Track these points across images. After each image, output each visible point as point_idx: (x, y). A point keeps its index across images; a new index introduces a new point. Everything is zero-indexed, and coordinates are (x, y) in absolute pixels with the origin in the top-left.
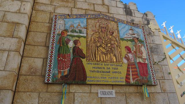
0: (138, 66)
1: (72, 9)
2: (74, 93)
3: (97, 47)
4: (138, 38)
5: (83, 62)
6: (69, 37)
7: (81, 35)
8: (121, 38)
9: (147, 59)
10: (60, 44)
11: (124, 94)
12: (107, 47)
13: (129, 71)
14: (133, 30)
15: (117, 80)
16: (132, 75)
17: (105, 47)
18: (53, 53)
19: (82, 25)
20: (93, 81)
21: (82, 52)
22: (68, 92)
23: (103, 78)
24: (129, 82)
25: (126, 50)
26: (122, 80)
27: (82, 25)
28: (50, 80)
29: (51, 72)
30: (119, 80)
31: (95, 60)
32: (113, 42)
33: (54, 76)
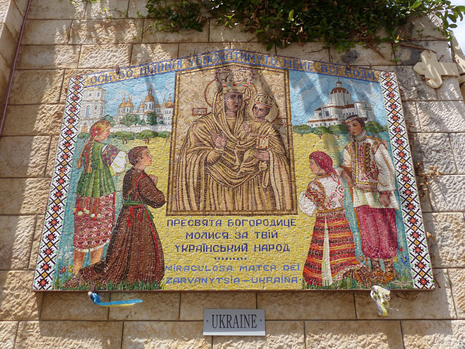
0: (358, 221)
1: (135, 46)
2: (124, 321)
3: (206, 164)
5: (154, 220)
6: (113, 142)
8: (296, 127)
10: (86, 163)
11: (298, 323)
12: (241, 160)
13: (321, 243)
14: (344, 90)
16: (332, 254)
17: (235, 161)
18: (63, 198)
20: (183, 280)
21: (155, 186)
22: (105, 319)
23: (222, 268)
24: (319, 282)
29: (53, 255)
30: (279, 272)
31: (195, 208)
32: (264, 143)
33: (62, 270)
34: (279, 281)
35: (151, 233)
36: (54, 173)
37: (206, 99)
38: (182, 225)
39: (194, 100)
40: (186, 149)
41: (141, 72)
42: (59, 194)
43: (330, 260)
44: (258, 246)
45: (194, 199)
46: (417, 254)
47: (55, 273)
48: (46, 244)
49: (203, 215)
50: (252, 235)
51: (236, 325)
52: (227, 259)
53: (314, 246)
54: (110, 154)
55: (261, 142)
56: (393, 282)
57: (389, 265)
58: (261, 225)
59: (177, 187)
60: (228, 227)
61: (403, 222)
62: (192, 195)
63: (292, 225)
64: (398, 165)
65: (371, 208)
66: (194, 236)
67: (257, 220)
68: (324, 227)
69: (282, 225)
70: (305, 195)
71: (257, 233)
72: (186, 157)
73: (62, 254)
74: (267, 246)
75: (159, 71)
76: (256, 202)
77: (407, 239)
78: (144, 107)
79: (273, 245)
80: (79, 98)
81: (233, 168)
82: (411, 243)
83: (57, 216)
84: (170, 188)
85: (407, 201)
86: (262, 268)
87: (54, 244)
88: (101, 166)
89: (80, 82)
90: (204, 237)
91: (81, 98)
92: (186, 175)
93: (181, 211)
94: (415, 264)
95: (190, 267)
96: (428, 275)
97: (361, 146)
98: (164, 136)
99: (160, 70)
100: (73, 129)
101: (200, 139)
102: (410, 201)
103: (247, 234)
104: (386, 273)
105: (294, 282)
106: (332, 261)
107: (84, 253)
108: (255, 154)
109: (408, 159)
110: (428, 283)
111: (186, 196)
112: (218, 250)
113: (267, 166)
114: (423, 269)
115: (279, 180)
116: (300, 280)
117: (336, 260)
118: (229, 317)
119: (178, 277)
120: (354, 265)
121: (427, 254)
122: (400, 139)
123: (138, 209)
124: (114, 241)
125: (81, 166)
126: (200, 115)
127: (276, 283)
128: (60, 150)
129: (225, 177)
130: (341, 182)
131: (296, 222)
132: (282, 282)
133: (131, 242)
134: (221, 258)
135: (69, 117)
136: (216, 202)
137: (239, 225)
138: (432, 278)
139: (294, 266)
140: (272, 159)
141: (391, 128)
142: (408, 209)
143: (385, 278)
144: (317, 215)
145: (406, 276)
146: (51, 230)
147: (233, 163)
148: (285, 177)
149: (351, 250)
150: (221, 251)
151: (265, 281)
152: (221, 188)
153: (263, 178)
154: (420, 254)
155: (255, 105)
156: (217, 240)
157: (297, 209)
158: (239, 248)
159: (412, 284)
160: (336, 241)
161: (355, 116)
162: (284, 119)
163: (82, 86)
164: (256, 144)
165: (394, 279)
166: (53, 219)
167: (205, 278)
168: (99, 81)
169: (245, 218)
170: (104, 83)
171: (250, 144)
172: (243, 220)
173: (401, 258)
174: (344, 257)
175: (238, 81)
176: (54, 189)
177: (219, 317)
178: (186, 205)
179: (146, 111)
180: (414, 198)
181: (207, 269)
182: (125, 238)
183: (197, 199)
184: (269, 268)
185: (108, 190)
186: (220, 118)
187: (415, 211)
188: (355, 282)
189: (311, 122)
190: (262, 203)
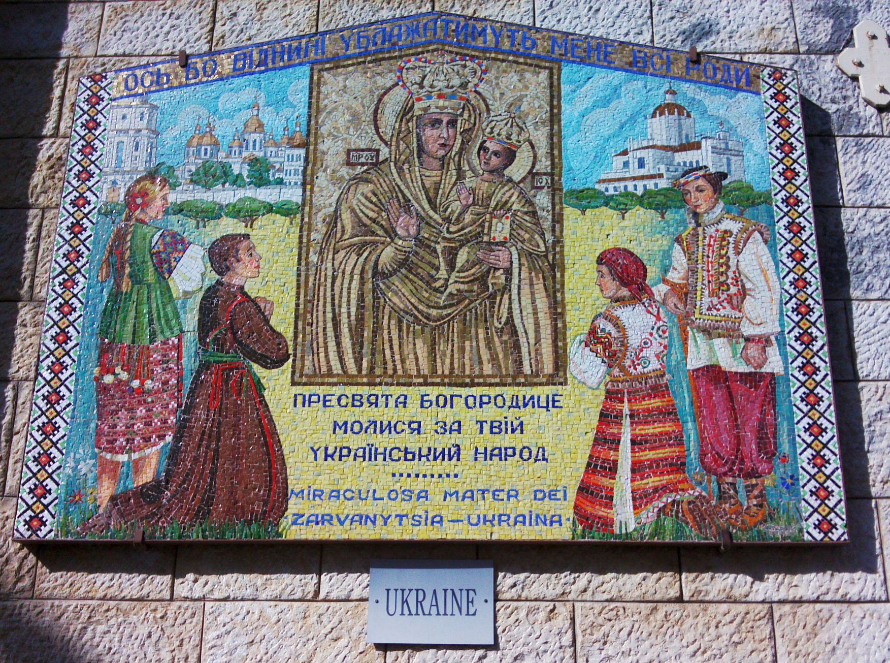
3: (375, 274)
4: (724, 176)
5: (266, 393)
6: (175, 223)
7: (266, 195)
8: (572, 192)
9: (781, 339)
10: (118, 273)
12: (451, 266)
13: (615, 442)
14: (681, 109)
15: (512, 508)
16: (637, 469)
17: (437, 269)
19: (274, 122)
21: (267, 321)
23: (408, 494)
24: (607, 523)
25: (608, 279)
26: (547, 507)
27: (274, 122)
28: (44, 524)
30: (524, 505)
33: (74, 496)
34: (524, 523)
35: (260, 421)
36: (50, 292)
37: (377, 128)
38: (325, 406)
39: (351, 131)
40: (333, 242)
41: (235, 64)
42: (62, 338)
43: (632, 481)
44: (481, 450)
45: (350, 351)
46: (816, 470)
47: (60, 502)
48: (39, 443)
49: (369, 384)
50: (469, 427)
51: (434, 609)
52: (417, 476)
53: (600, 452)
54: (169, 250)
55: (493, 228)
56: (762, 528)
57: (756, 492)
58: (490, 405)
59: (314, 326)
60: (420, 410)
61: (790, 401)
62: (346, 342)
63: (554, 406)
64: (787, 280)
65: (725, 372)
66: (349, 429)
67: (481, 397)
68: (621, 410)
69: (533, 407)
70: (583, 344)
71: (481, 423)
72: (333, 259)
73: (73, 464)
74: (500, 449)
75: (274, 63)
76: (480, 358)
77: (798, 439)
78: (241, 146)
79: (514, 449)
80: (99, 125)
81: (433, 285)
82: (805, 446)
83: (59, 383)
84: (300, 327)
85: (803, 357)
86: (488, 496)
87: (54, 444)
88: (151, 277)
89: (102, 88)
90: (371, 430)
91: (105, 125)
92: (333, 299)
93: (323, 376)
94: (811, 491)
95: (342, 493)
96: (836, 513)
97: (711, 237)
98: (285, 210)
99: (277, 59)
100: (88, 194)
101: (365, 219)
102: (808, 357)
103: (459, 425)
104: (749, 508)
105: (556, 525)
106: (636, 483)
107: (118, 463)
108: (480, 255)
109: (811, 266)
110: (834, 530)
111: (334, 343)
112: (400, 459)
113: (506, 279)
114: (827, 501)
115: (530, 310)
116: (568, 519)
117: (645, 481)
118: (421, 594)
119: (317, 512)
120: (683, 490)
121: (837, 468)
122: (797, 221)
123: (231, 370)
124: (182, 436)
125: (108, 276)
126: (363, 164)
127: (517, 527)
128: (61, 240)
129: (416, 304)
130: (662, 315)
131: (562, 401)
132: (537, 524)
133: (219, 440)
134: (405, 475)
135: (78, 167)
136: (397, 357)
137: (444, 406)
138: (843, 520)
139: (556, 491)
140: (516, 265)
141: (779, 197)
142: (804, 375)
143: (747, 518)
144: (609, 386)
145: (791, 513)
146: (47, 414)
147: (433, 272)
148: (542, 303)
149: (677, 461)
150: (406, 459)
151: (496, 522)
152: (408, 327)
153: (496, 306)
154: (823, 469)
155: (485, 142)
156: (397, 436)
157: (565, 374)
158: (443, 453)
159: (801, 530)
160: (646, 442)
161: (701, 168)
162: (545, 174)
163: (107, 96)
164: (483, 231)
165: (766, 521)
166: (50, 390)
167: (372, 516)
168: (143, 84)
169: (456, 391)
170: (153, 89)
171: (470, 232)
172: (452, 396)
173: (782, 478)
174: (662, 474)
175: (447, 87)
176: (52, 326)
177: (399, 592)
178: (332, 363)
179: (245, 154)
180: (818, 351)
181: (377, 496)
182: (204, 432)
183: (358, 349)
184: (503, 495)
185: (166, 329)
186: (406, 171)
187: (818, 379)
188: (681, 526)
189: (604, 181)
190: (494, 359)
